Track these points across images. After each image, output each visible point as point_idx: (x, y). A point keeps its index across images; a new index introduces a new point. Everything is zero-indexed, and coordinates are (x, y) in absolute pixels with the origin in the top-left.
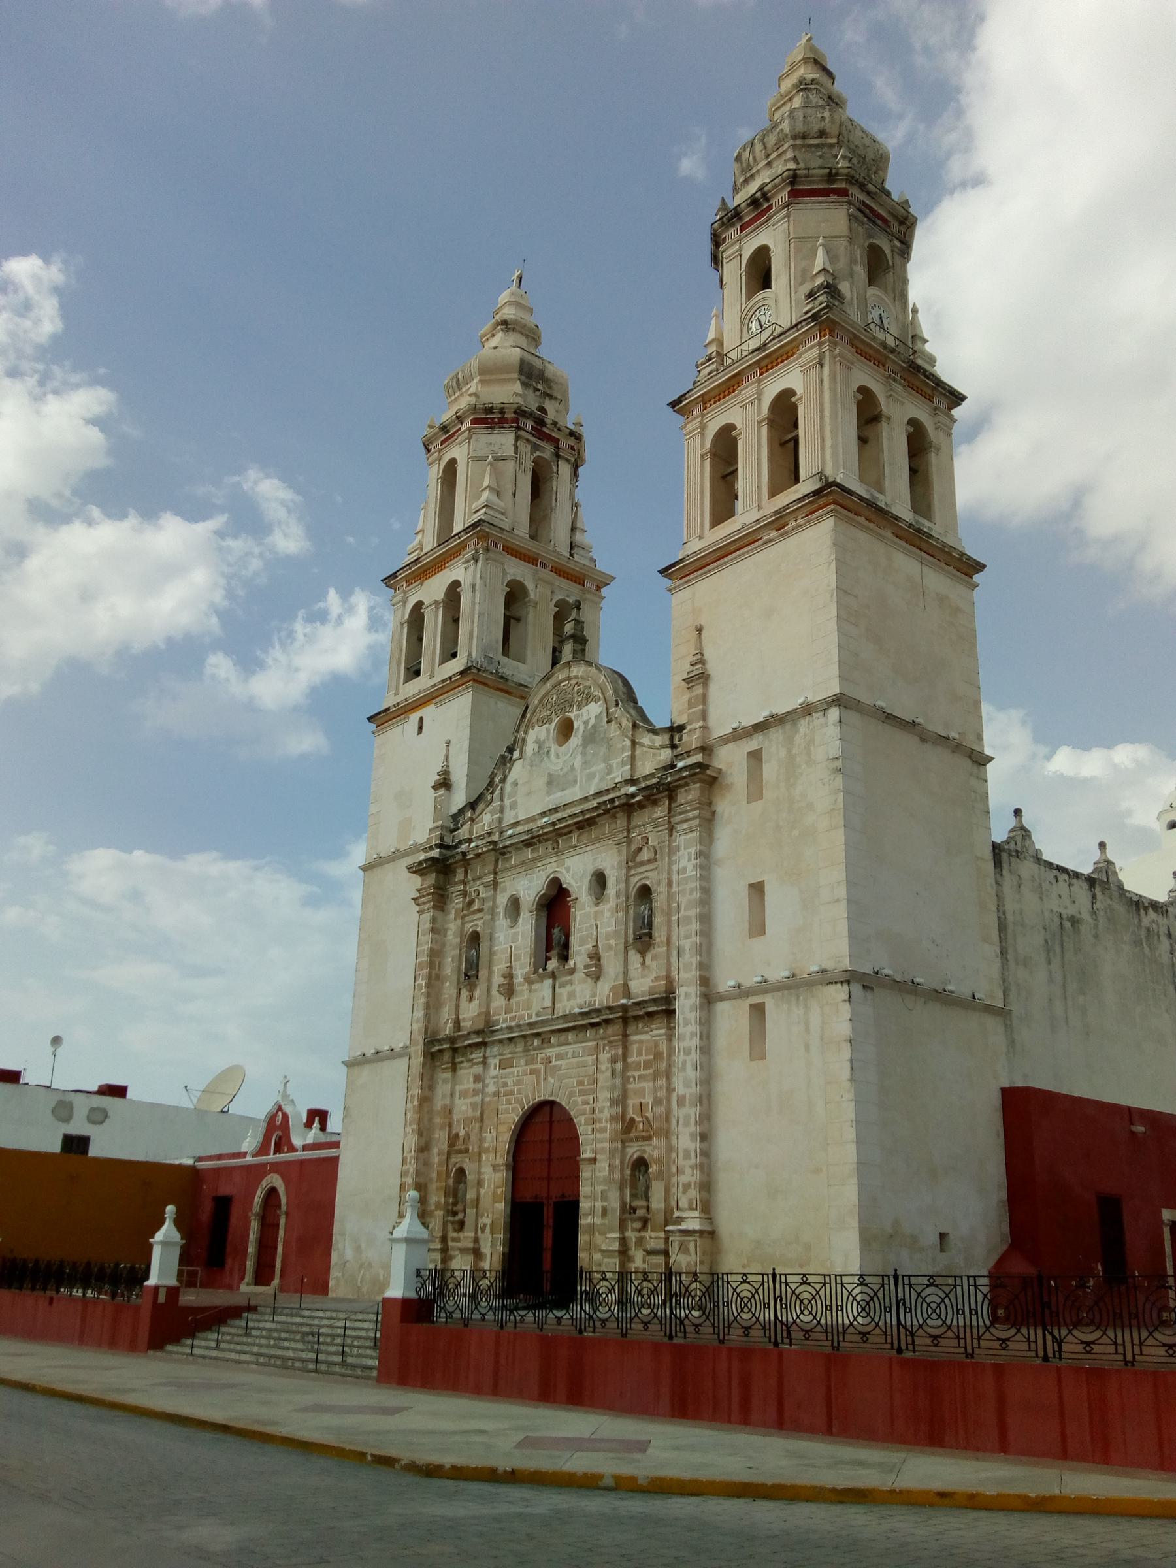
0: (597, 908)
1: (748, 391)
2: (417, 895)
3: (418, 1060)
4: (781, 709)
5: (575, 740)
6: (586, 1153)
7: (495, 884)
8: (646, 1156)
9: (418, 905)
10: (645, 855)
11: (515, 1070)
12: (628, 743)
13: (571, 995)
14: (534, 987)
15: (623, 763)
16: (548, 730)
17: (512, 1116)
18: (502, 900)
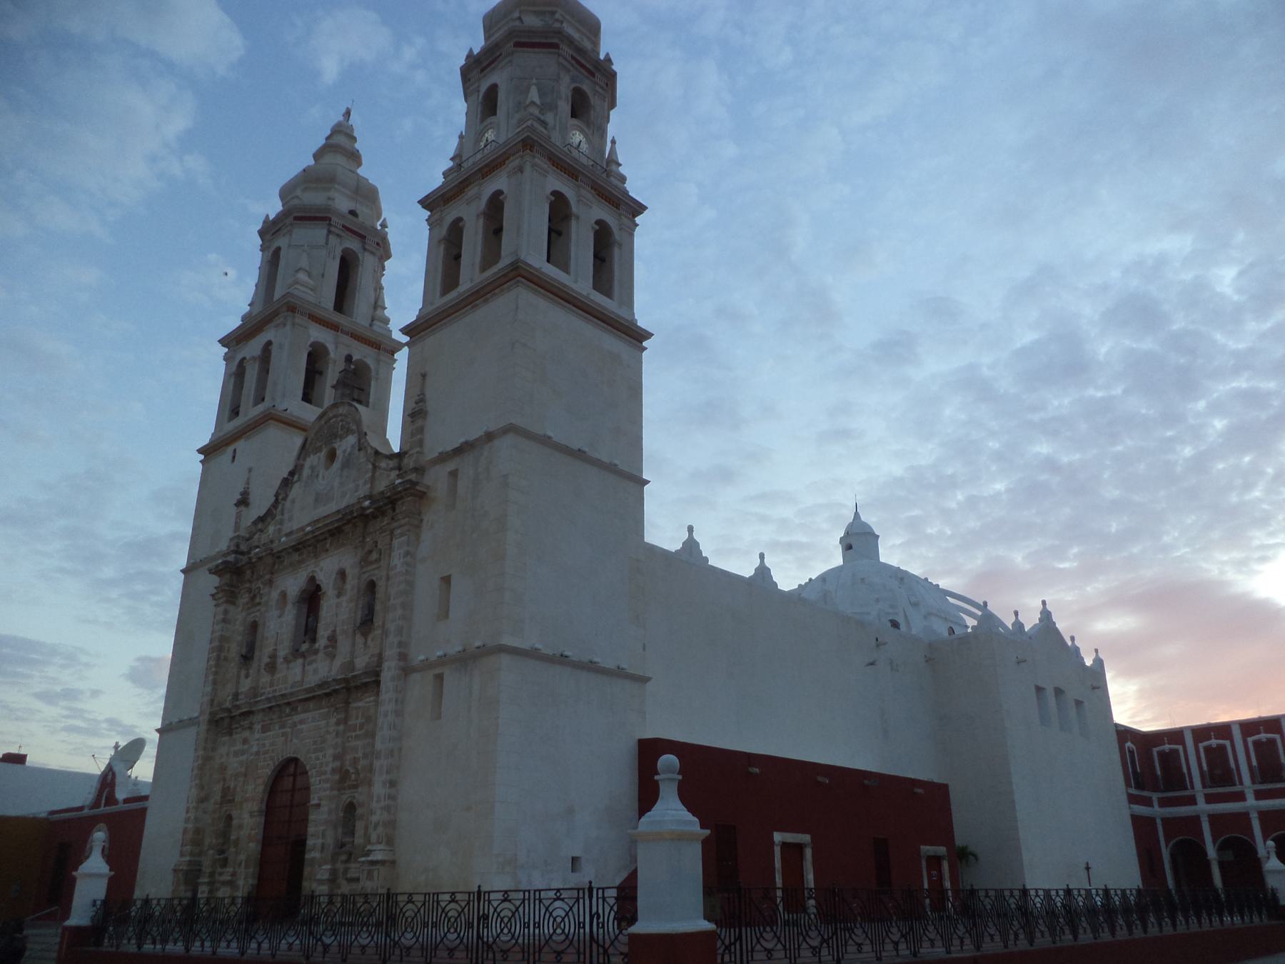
0: (338, 600)
1: (471, 192)
2: (215, 591)
3: (204, 727)
5: (337, 465)
7: (271, 582)
8: (355, 801)
9: (215, 600)
10: (374, 556)
11: (272, 733)
12: (370, 466)
13: (316, 671)
14: (292, 665)
15: (365, 483)
16: (319, 458)
17: (266, 770)
18: (275, 595)
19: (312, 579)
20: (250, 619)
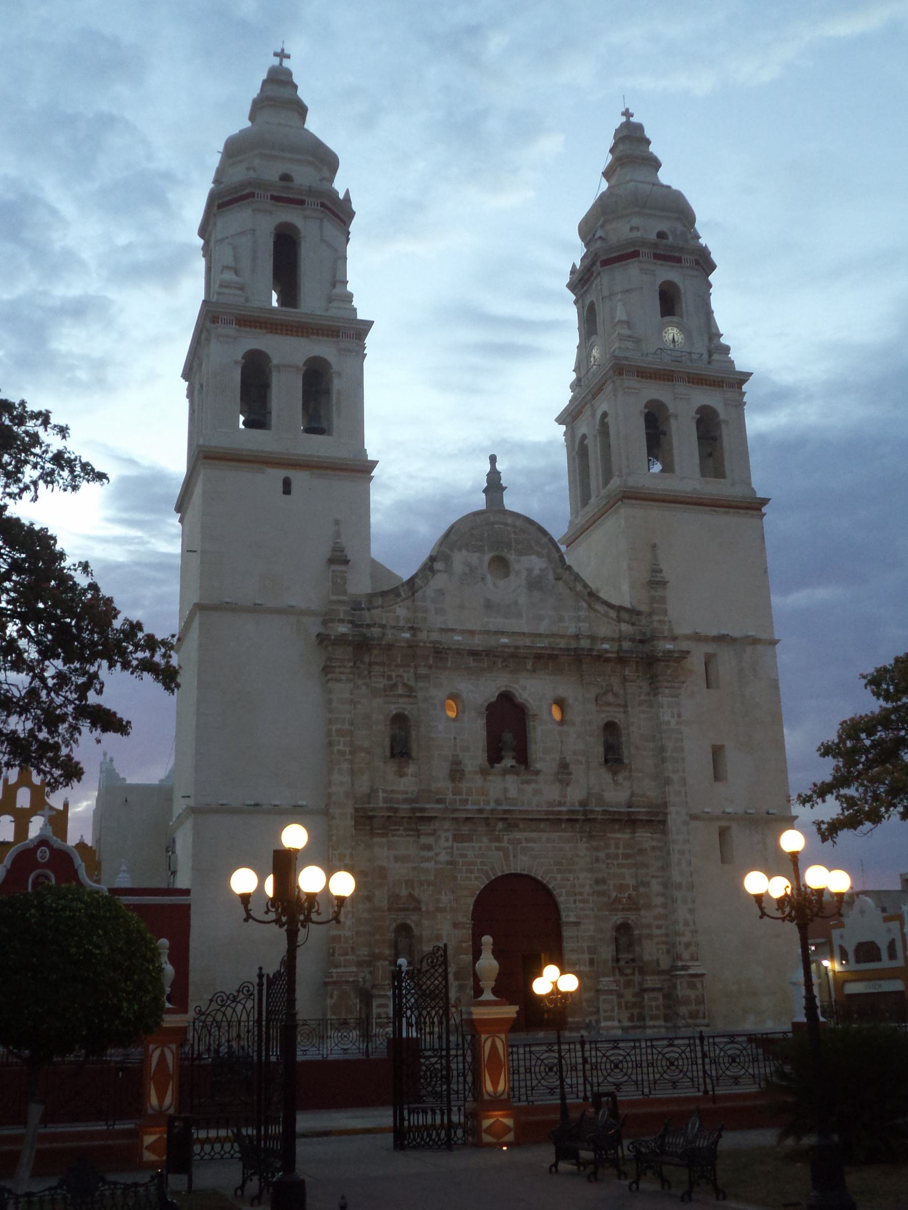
4: (735, 634)
6: (568, 916)
8: (630, 922)
19: (506, 698)
20: (393, 709)
